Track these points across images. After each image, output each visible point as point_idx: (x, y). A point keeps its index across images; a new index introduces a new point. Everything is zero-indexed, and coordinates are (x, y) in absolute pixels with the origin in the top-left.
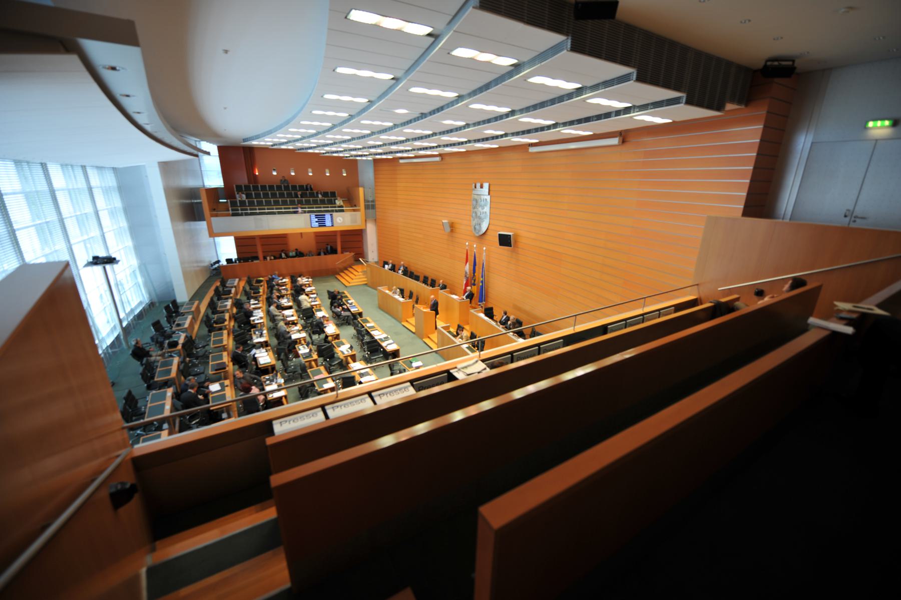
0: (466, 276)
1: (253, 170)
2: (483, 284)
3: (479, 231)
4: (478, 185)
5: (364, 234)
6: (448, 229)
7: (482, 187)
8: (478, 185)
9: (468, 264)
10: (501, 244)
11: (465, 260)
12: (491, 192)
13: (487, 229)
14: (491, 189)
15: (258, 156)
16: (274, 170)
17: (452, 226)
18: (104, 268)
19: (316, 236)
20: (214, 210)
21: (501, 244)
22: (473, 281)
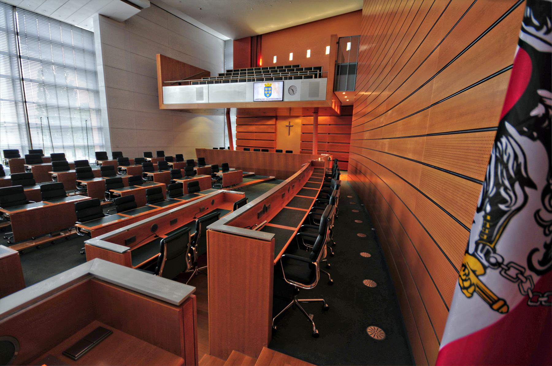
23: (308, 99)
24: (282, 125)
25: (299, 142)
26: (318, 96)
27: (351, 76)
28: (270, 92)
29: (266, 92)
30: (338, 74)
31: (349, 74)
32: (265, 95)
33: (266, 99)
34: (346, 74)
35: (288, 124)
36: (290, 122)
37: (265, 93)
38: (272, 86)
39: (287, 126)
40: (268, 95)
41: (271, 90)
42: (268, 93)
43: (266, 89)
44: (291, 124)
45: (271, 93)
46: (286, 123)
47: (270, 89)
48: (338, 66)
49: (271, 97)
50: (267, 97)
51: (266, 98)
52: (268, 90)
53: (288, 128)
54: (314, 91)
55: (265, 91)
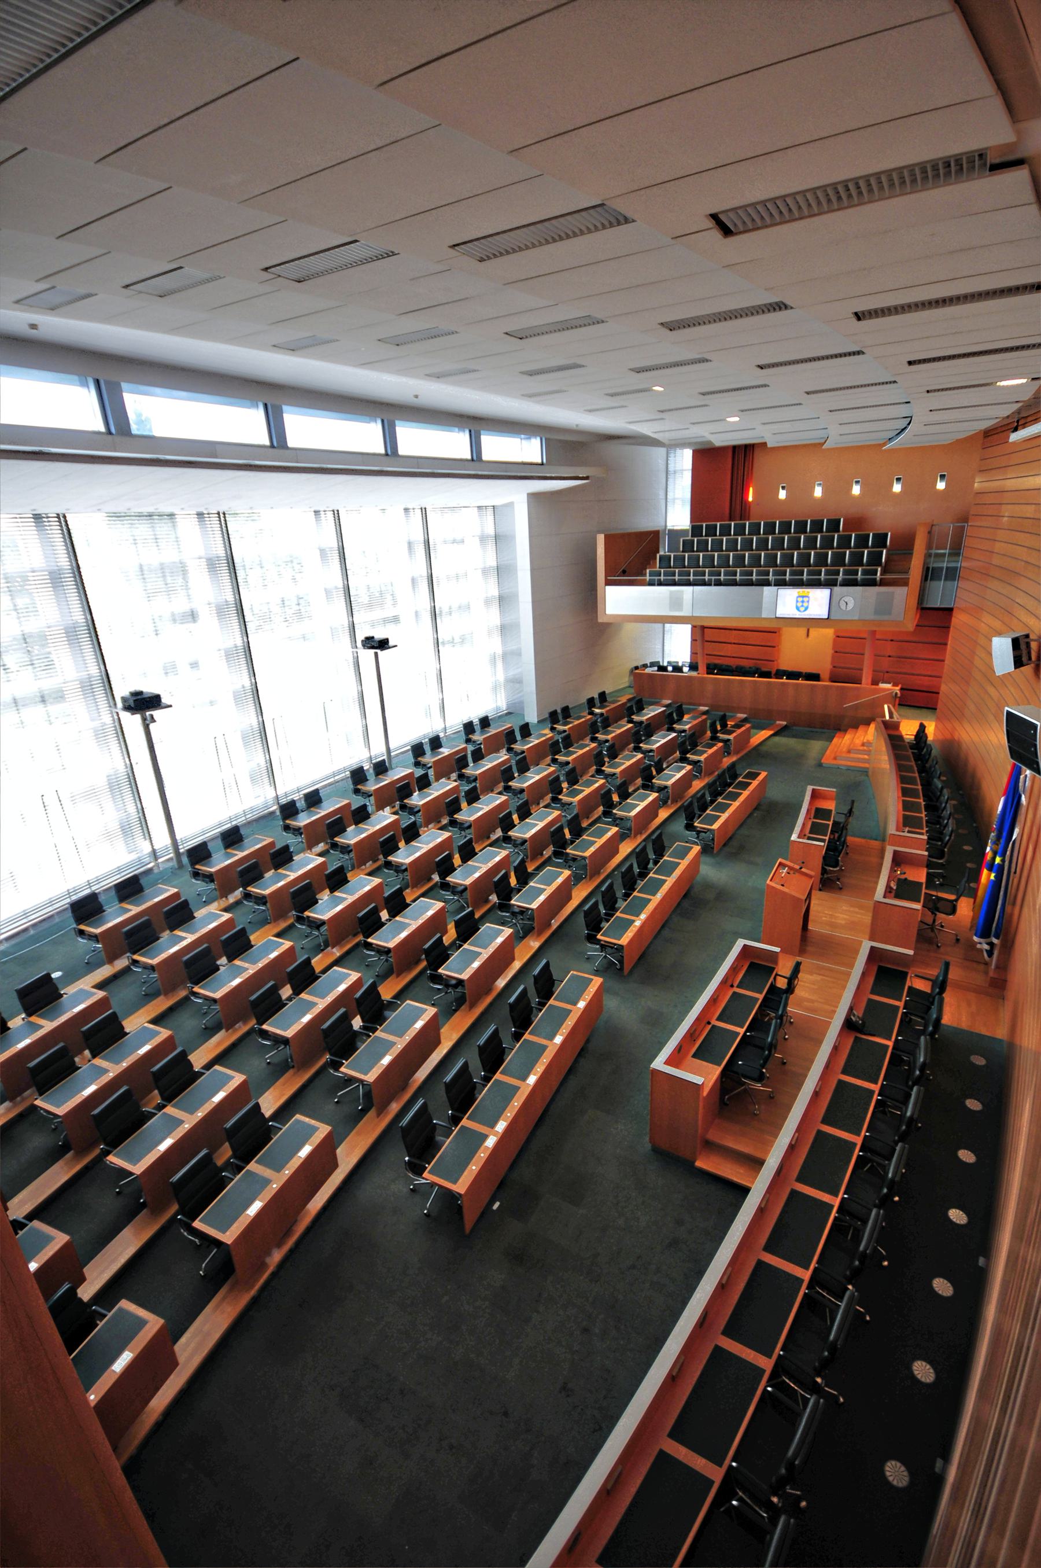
1: (744, 493)
16: (783, 488)
18: (376, 654)
20: (624, 572)
23: (870, 616)
25: (830, 651)
26: (890, 614)
27: (949, 583)
29: (800, 604)
30: (926, 579)
31: (946, 579)
32: (798, 608)
33: (798, 615)
34: (941, 580)
38: (810, 595)
40: (802, 609)
43: (800, 599)
47: (806, 599)
48: (928, 568)
49: (807, 612)
51: (798, 613)
54: (883, 607)
55: (797, 601)
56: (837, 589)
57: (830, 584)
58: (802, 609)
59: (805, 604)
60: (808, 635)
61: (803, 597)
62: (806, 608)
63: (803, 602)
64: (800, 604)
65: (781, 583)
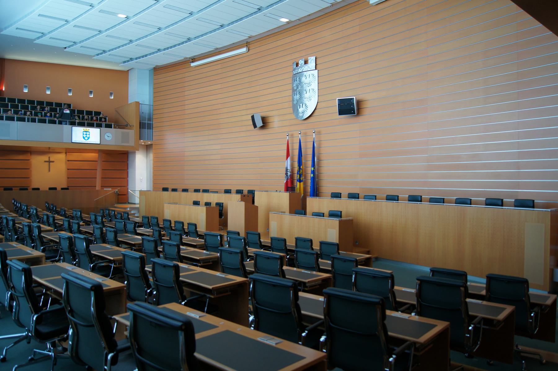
0: (286, 174)
2: (314, 175)
3: (303, 112)
4: (301, 62)
5: (130, 171)
6: (259, 123)
7: (306, 62)
8: (301, 62)
9: (289, 158)
10: (341, 112)
11: (285, 154)
12: (318, 66)
13: (315, 109)
14: (317, 63)
15: (9, 70)
17: (264, 119)
19: (68, 169)
21: (341, 112)
22: (298, 176)
24: (37, 162)
27: (149, 130)
28: (88, 136)
32: (84, 138)
35: (47, 160)
36: (49, 157)
37: (83, 137)
39: (45, 161)
40: (86, 138)
41: (89, 134)
42: (86, 137)
43: (85, 133)
44: (51, 160)
45: (89, 137)
46: (45, 158)
47: (88, 133)
50: (85, 139)
52: (86, 134)
53: (47, 163)
55: (83, 134)
56: (104, 129)
57: (99, 126)
58: (86, 138)
59: (88, 136)
60: (49, 171)
61: (86, 132)
62: (89, 138)
63: (86, 134)
64: (85, 136)
65: (73, 124)
